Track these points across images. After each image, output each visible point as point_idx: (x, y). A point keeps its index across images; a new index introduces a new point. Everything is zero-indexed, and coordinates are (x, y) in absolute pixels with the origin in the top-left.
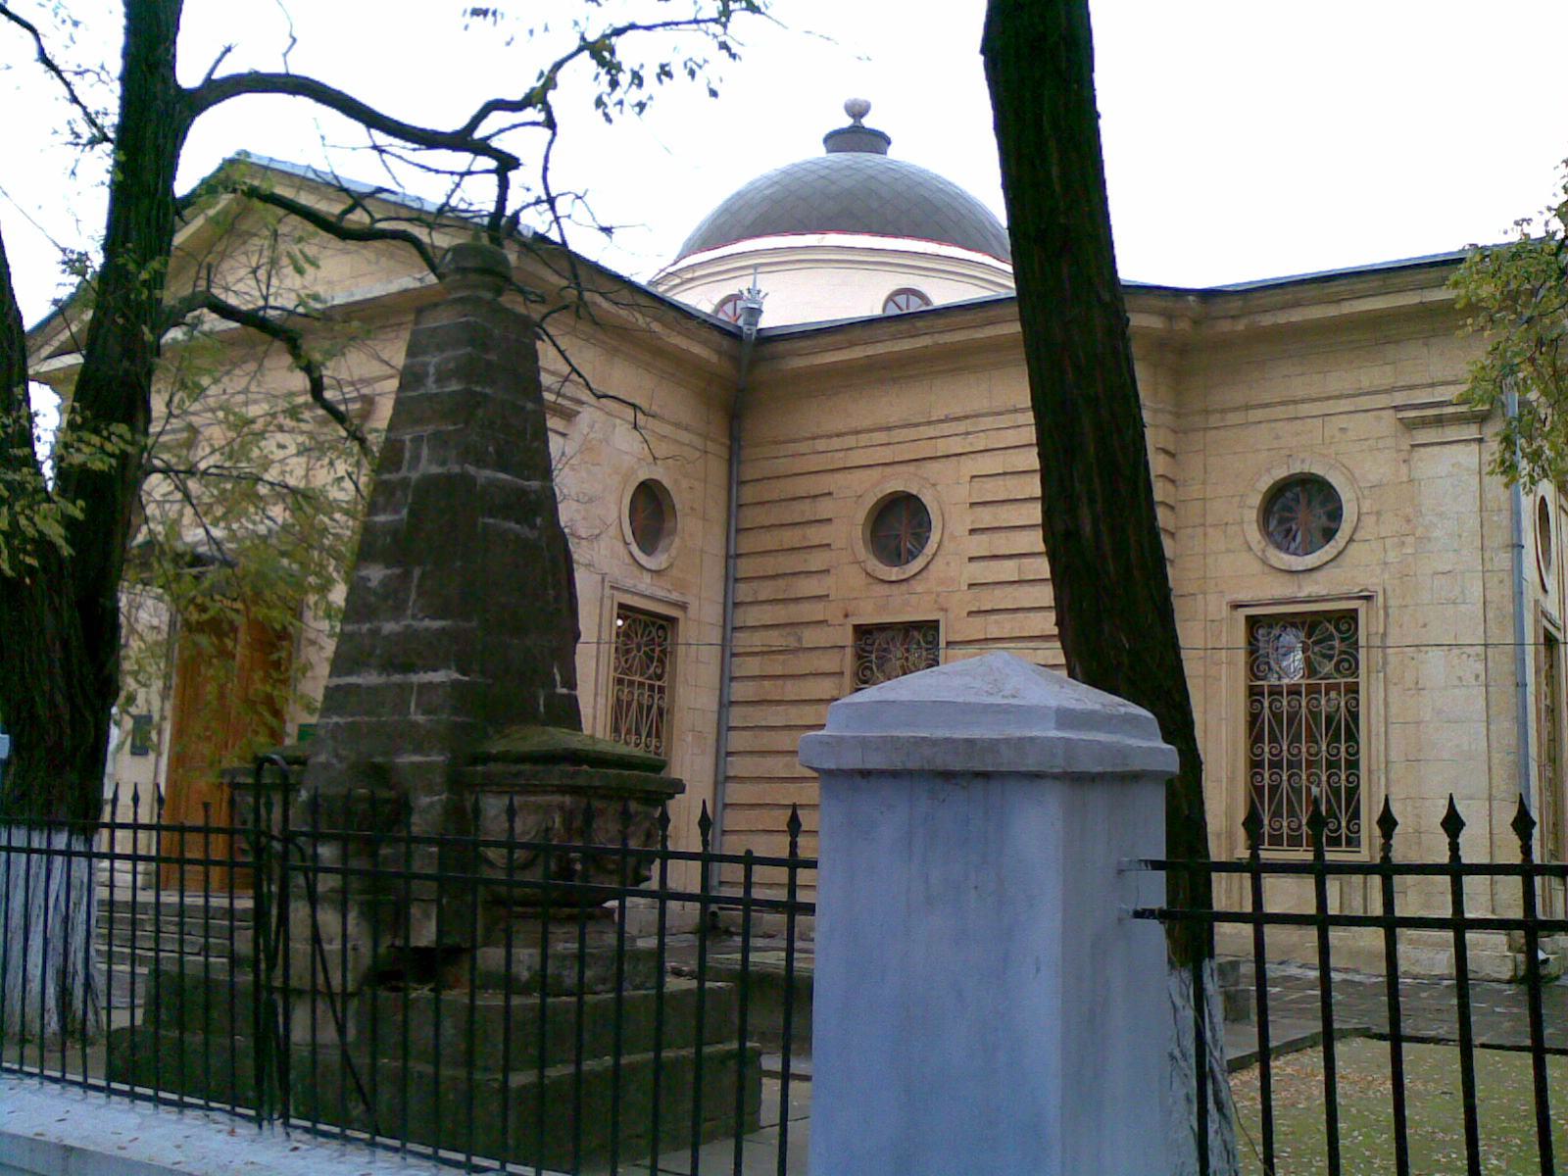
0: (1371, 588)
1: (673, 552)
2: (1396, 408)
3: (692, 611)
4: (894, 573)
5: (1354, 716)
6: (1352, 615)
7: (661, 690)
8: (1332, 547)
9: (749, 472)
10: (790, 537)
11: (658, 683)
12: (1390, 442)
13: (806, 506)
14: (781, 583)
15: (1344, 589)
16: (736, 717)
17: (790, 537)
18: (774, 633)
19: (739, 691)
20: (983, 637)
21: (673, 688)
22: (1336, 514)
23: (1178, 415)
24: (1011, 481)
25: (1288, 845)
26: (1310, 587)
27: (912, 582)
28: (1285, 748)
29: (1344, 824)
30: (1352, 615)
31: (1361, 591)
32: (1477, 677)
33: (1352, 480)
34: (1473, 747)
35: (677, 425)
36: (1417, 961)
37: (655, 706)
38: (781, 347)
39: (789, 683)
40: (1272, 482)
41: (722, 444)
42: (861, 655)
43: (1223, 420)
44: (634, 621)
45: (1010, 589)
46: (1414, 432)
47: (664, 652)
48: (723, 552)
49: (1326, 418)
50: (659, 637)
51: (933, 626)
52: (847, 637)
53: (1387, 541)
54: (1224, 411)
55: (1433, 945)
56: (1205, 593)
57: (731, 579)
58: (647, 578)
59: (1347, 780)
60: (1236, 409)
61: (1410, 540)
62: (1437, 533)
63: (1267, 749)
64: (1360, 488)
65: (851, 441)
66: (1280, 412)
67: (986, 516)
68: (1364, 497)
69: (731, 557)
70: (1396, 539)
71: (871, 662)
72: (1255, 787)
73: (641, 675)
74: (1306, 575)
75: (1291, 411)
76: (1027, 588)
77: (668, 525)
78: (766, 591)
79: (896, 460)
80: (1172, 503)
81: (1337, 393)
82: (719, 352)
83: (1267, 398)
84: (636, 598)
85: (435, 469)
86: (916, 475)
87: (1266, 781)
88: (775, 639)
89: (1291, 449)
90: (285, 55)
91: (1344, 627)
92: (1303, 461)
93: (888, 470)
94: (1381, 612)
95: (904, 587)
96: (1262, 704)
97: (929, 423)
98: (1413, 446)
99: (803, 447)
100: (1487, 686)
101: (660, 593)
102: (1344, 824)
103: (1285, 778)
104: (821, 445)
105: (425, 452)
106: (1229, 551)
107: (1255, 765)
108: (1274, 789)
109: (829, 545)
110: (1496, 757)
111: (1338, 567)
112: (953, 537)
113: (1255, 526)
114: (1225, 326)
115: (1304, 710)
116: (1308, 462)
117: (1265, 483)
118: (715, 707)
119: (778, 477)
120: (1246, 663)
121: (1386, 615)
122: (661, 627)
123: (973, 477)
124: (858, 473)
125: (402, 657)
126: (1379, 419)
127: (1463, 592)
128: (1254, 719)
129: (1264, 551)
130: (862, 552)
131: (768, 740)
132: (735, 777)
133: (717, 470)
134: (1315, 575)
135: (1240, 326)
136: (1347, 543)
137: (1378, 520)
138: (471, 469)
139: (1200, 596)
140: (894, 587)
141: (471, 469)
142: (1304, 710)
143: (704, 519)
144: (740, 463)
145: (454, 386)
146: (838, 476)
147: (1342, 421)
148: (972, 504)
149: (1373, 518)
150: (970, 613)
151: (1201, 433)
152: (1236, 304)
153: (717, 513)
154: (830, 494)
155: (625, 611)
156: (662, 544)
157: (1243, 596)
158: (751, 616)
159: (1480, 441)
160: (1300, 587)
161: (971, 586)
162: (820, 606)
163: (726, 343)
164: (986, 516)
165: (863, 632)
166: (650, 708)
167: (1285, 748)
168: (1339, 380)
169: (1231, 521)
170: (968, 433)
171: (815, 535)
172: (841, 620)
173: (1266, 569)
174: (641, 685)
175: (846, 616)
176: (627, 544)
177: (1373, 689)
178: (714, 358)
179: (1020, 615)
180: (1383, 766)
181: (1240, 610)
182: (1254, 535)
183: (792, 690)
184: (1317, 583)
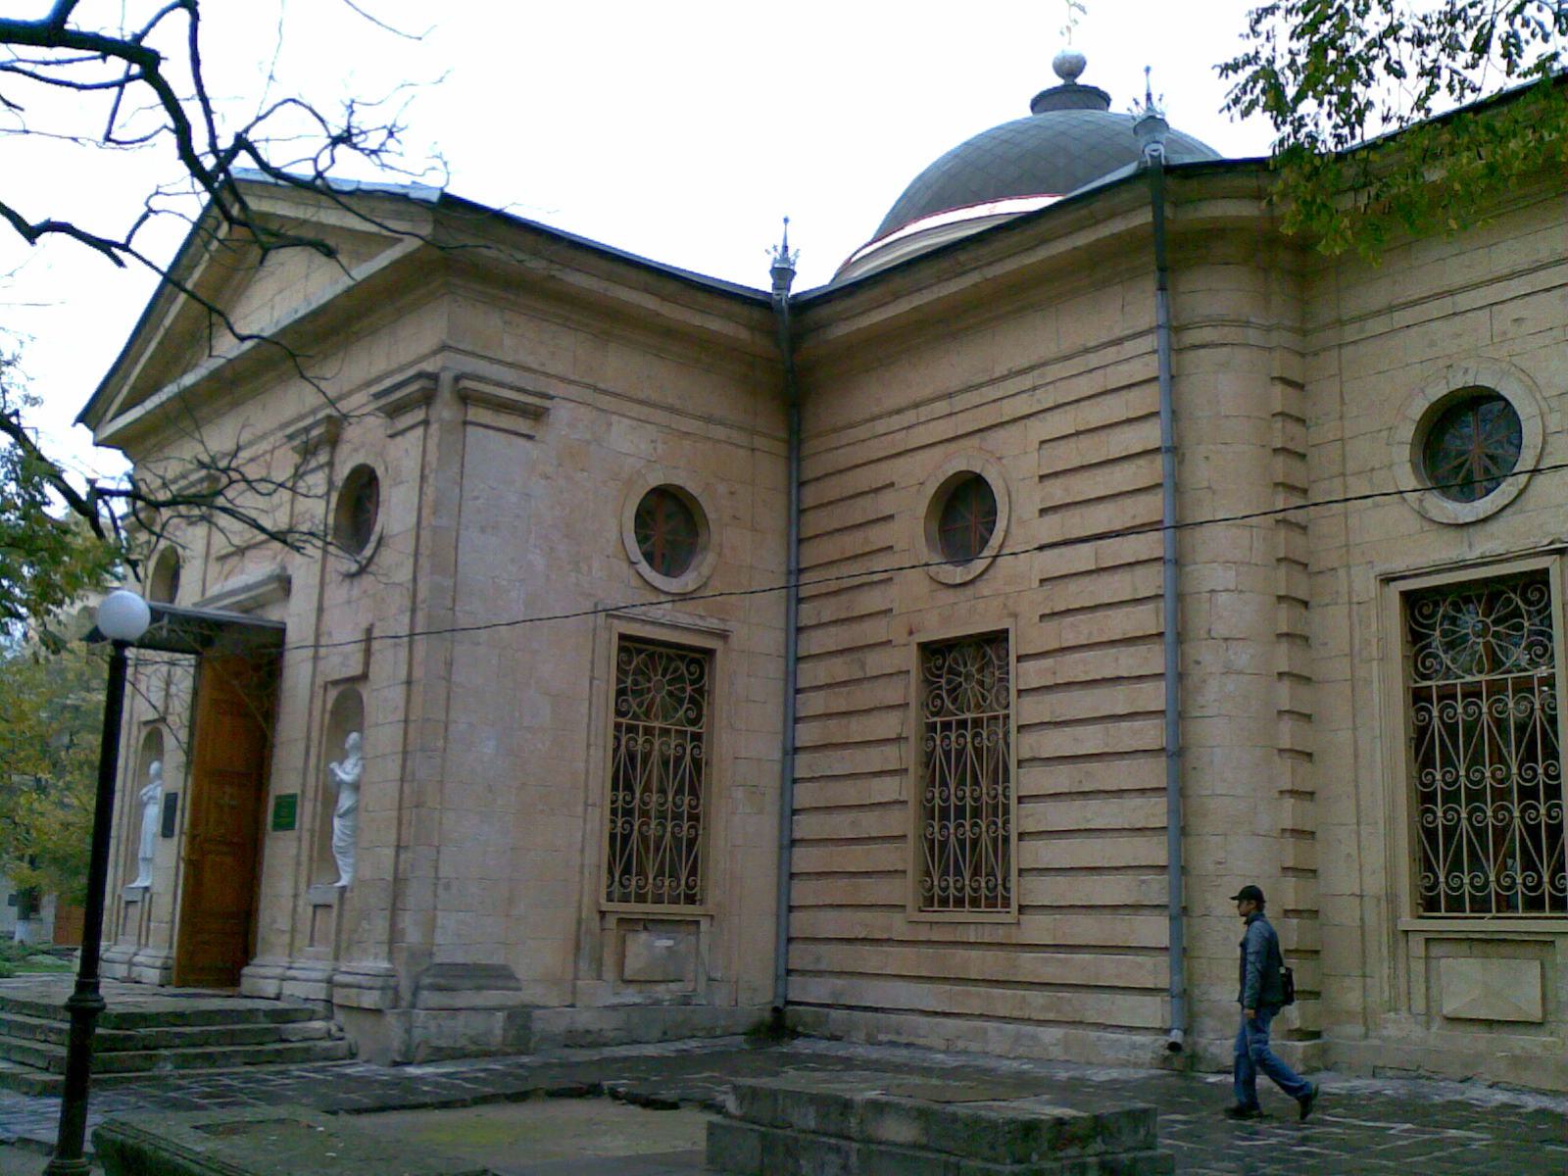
3: (734, 640)
4: (959, 574)
5: (1553, 721)
6: (1540, 578)
8: (1510, 485)
9: (811, 470)
10: (852, 543)
11: (690, 729)
16: (803, 765)
17: (852, 543)
18: (839, 660)
19: (806, 734)
20: (1056, 646)
24: (1085, 442)
25: (1472, 911)
27: (978, 584)
28: (1462, 773)
29: (1546, 879)
31: (1551, 543)
35: (709, 419)
37: (688, 758)
38: (825, 312)
41: (776, 439)
42: (930, 680)
43: (1362, 331)
44: (651, 656)
45: (1086, 580)
47: (700, 691)
48: (783, 568)
49: (1495, 308)
50: (691, 674)
51: (999, 638)
52: (909, 659)
54: (1362, 318)
56: (1349, 567)
59: (1495, 817)
60: (1379, 313)
63: (1438, 776)
64: (1545, 398)
65: (910, 417)
66: (1434, 308)
67: (1057, 491)
68: (1551, 410)
71: (940, 688)
73: (665, 718)
74: (1479, 527)
75: (1447, 305)
76: (1106, 577)
77: (702, 540)
78: (829, 610)
79: (959, 433)
80: (1301, 450)
81: (1506, 271)
82: (752, 329)
84: (648, 628)
86: (981, 448)
87: (1440, 821)
88: (839, 669)
89: (1449, 356)
91: (1534, 596)
92: (1466, 371)
93: (952, 446)
95: (970, 591)
96: (1430, 712)
97: (993, 382)
101: (684, 619)
102: (1546, 879)
103: (1464, 815)
104: (881, 427)
109: (891, 547)
111: (1522, 511)
112: (1022, 522)
117: (1418, 408)
118: (777, 755)
119: (841, 472)
120: (1405, 657)
122: (693, 661)
123: (1043, 442)
128: (1420, 737)
131: (850, 793)
132: (802, 840)
133: (771, 471)
139: (1342, 573)
140: (960, 592)
143: (754, 530)
148: (1042, 478)
150: (1042, 617)
151: (1334, 353)
153: (773, 517)
154: (892, 484)
155: (629, 645)
156: (695, 562)
157: (1398, 565)
160: (1470, 546)
161: (1042, 581)
162: (883, 621)
163: (757, 314)
164: (1057, 491)
165: (934, 652)
166: (679, 760)
167: (1462, 773)
168: (1511, 251)
169: (1377, 466)
170: (1034, 389)
171: (877, 536)
172: (903, 638)
173: (1427, 526)
174: (665, 732)
175: (911, 633)
178: (744, 334)
179: (1099, 614)
181: (1392, 584)
183: (857, 729)
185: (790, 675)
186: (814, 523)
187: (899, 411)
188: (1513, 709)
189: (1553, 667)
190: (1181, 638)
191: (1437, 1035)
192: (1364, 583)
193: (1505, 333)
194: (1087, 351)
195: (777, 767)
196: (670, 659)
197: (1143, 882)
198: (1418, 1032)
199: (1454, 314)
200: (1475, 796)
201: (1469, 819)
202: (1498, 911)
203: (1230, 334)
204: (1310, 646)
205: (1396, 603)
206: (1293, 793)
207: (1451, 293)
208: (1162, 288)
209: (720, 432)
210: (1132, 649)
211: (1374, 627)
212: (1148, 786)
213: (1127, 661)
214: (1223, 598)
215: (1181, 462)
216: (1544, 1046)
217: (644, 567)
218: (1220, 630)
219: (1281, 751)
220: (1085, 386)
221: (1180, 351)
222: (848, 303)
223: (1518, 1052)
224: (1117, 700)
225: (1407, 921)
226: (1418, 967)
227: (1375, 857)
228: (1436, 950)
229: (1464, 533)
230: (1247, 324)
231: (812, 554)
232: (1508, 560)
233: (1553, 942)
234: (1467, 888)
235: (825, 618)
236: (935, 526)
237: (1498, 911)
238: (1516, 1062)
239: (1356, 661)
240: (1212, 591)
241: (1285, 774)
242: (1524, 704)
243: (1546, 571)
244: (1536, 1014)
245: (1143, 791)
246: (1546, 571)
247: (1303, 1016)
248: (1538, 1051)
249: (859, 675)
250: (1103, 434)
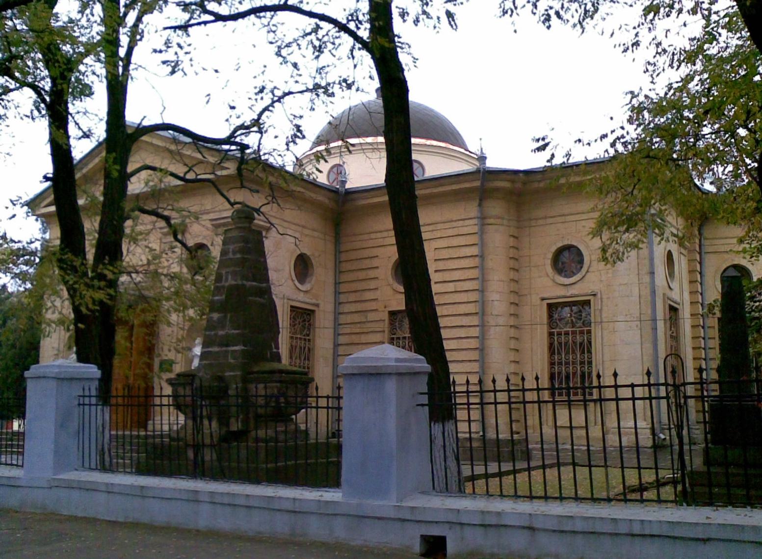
1: (313, 282)
3: (321, 306)
5: (590, 343)
6: (588, 303)
7: (309, 340)
9: (343, 248)
10: (362, 275)
13: (367, 261)
14: (358, 294)
15: (585, 291)
18: (356, 315)
21: (314, 340)
22: (581, 262)
23: (518, 221)
30: (588, 303)
33: (587, 247)
35: (314, 230)
38: (355, 196)
39: (363, 336)
45: (451, 295)
47: (310, 325)
48: (334, 281)
52: (386, 316)
57: (337, 293)
58: (302, 294)
69: (337, 284)
73: (301, 334)
78: (352, 297)
82: (329, 199)
85: (233, 282)
88: (356, 318)
90: (161, 114)
99: (366, 237)
100: (641, 329)
101: (308, 300)
104: (373, 236)
105: (230, 277)
107: (552, 364)
110: (645, 358)
114: (536, 185)
115: (570, 341)
117: (554, 249)
118: (332, 346)
119: (355, 250)
121: (602, 301)
122: (309, 314)
124: (389, 247)
125: (226, 342)
127: (631, 292)
128: (551, 346)
130: (391, 280)
133: (330, 247)
134: (573, 286)
135: (542, 185)
138: (245, 282)
139: (529, 296)
141: (245, 282)
142: (570, 341)
144: (339, 243)
145: (238, 256)
146: (380, 249)
148: (435, 260)
152: (539, 176)
153: (331, 264)
154: (377, 256)
155: (293, 307)
156: (308, 280)
157: (545, 296)
158: (346, 308)
162: (374, 303)
163: (332, 195)
166: (305, 348)
170: (433, 231)
171: (372, 273)
172: (384, 309)
175: (385, 307)
176: (293, 280)
178: (327, 201)
179: (456, 305)
182: (549, 269)
185: (336, 319)
186: (345, 266)
187: (381, 232)
188: (579, 339)
190: (483, 315)
192: (535, 299)
194: (452, 221)
195: (332, 351)
196: (302, 314)
200: (567, 363)
203: (499, 221)
205: (545, 307)
206: (514, 362)
208: (480, 205)
209: (316, 234)
210: (466, 317)
213: (465, 321)
214: (496, 303)
217: (296, 282)
218: (495, 312)
220: (450, 232)
222: (366, 194)
224: (462, 333)
229: (566, 287)
230: (503, 218)
231: (344, 277)
235: (350, 300)
236: (394, 271)
241: (512, 356)
242: (582, 338)
243: (589, 301)
245: (470, 361)
246: (589, 301)
249: (365, 320)
250: (457, 249)
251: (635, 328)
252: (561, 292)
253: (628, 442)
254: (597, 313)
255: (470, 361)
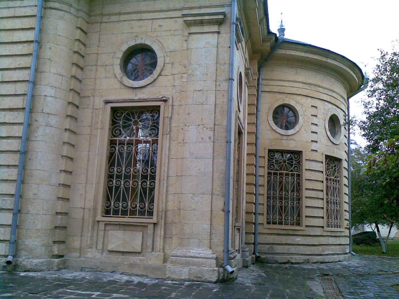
0: (167, 96)
2: (184, 16)
8: (152, 77)
12: (180, 32)
15: (155, 97)
22: (154, 65)
23: (90, 16)
26: (141, 95)
28: (124, 169)
30: (156, 109)
32: (210, 138)
34: (206, 170)
36: (174, 272)
40: (128, 47)
43: (109, 19)
46: (190, 27)
49: (154, 20)
53: (176, 76)
54: (109, 15)
55: (182, 264)
56: (94, 96)
60: (116, 14)
61: (185, 75)
62: (198, 73)
63: (115, 170)
64: (166, 52)
66: (134, 16)
70: (179, 75)
72: (109, 187)
74: (139, 90)
75: (138, 16)
80: (83, 54)
81: (159, 9)
83: (129, 10)
87: (114, 184)
89: (137, 33)
92: (142, 38)
94: (170, 107)
96: (115, 148)
98: (190, 34)
100: (214, 142)
103: (122, 183)
106: (106, 77)
107: (110, 177)
108: (117, 188)
110: (216, 175)
113: (119, 66)
116: (144, 39)
117: (125, 47)
120: (110, 129)
121: (173, 108)
126: (176, 22)
127: (206, 100)
128: (111, 156)
129: (122, 78)
136: (158, 76)
137: (172, 66)
139: (91, 98)
147: (160, 22)
149: (170, 66)
151: (99, 24)
159: (218, 33)
160: (136, 95)
167: (124, 169)
169: (108, 64)
173: (122, 87)
177: (164, 142)
180: (166, 178)
181: (108, 104)
182: (118, 70)
184: (144, 93)
189: (158, 137)
190: (31, 111)
191: (105, 257)
192: (99, 102)
193: (156, 29)
197: (4, 200)
198: (98, 255)
199: (141, 20)
201: (124, 185)
202: (130, 215)
203: (65, 7)
204: (77, 122)
206: (65, 171)
207: (140, 12)
210: (11, 113)
211: (100, 117)
212: (11, 164)
214: (49, 99)
215: (40, 48)
216: (140, 260)
218: (46, 110)
219: (62, 156)
221: (45, 8)
223: (132, 262)
225: (99, 218)
226: (101, 233)
227: (91, 196)
228: (108, 228)
229: (134, 91)
230: (71, 6)
232: (147, 101)
233: (147, 226)
234: (121, 207)
237: (130, 215)
238: (131, 266)
239: (93, 128)
240: (45, 96)
241: (63, 164)
243: (159, 107)
244: (139, 250)
245: (8, 166)
246: (159, 107)
247: (58, 250)
248: (138, 262)
250: (11, 33)
251: (208, 140)
252: (127, 95)
253: (190, 274)
254: (167, 121)
255: (8, 166)
